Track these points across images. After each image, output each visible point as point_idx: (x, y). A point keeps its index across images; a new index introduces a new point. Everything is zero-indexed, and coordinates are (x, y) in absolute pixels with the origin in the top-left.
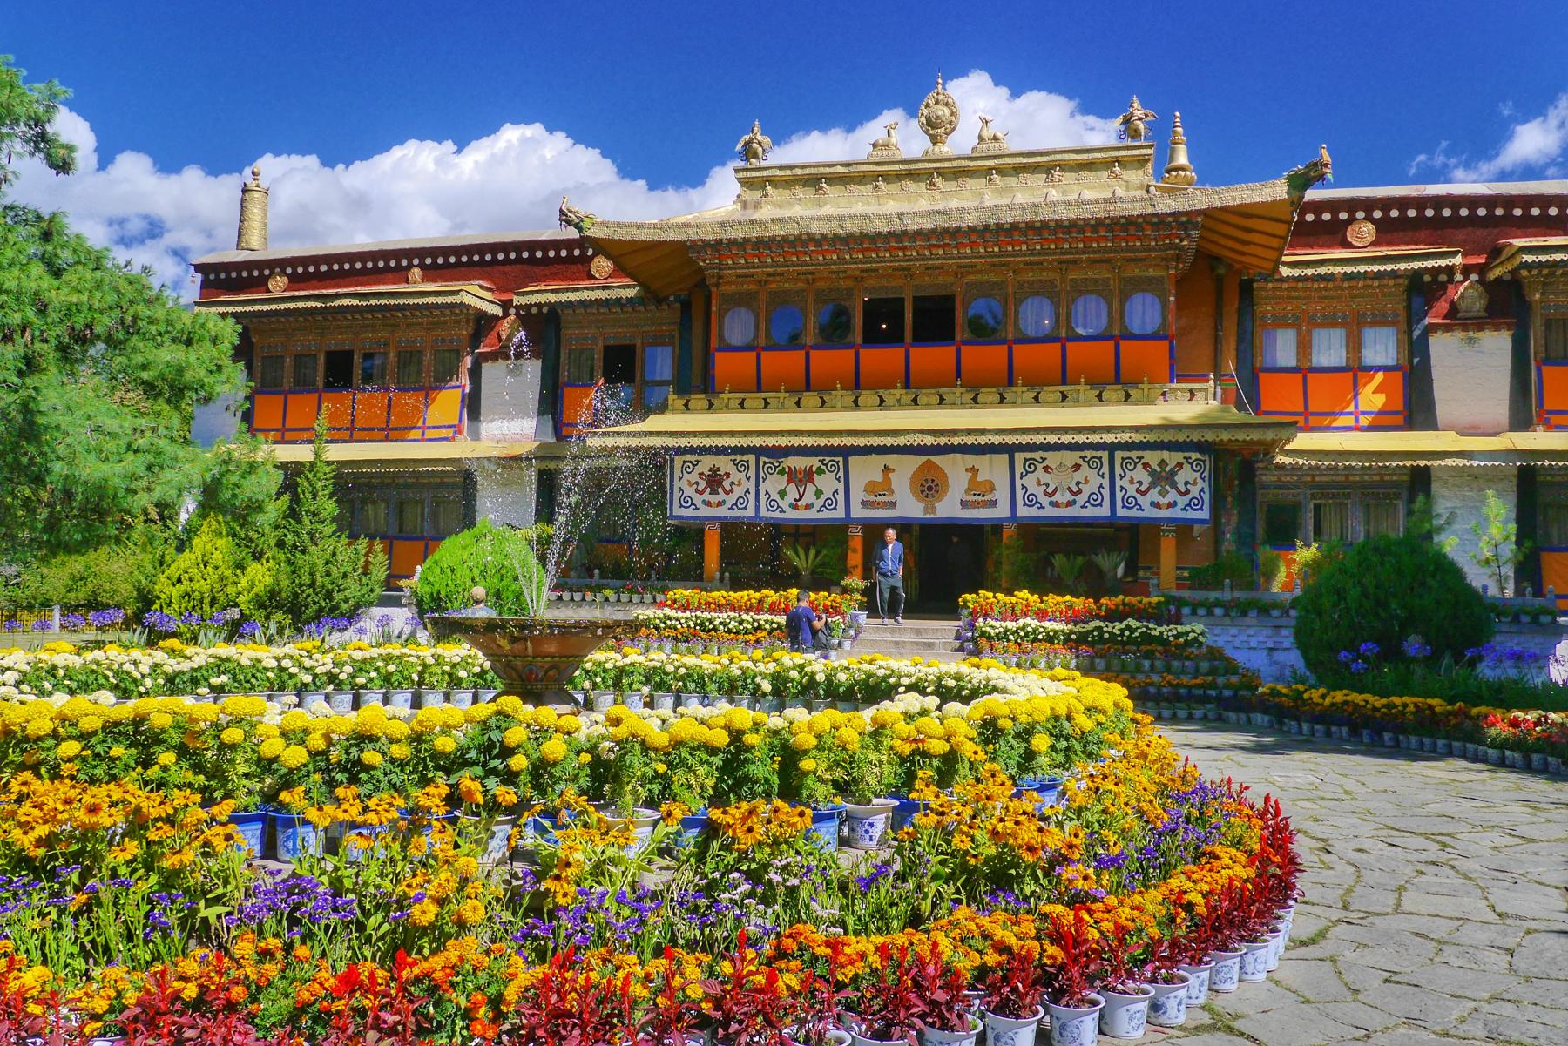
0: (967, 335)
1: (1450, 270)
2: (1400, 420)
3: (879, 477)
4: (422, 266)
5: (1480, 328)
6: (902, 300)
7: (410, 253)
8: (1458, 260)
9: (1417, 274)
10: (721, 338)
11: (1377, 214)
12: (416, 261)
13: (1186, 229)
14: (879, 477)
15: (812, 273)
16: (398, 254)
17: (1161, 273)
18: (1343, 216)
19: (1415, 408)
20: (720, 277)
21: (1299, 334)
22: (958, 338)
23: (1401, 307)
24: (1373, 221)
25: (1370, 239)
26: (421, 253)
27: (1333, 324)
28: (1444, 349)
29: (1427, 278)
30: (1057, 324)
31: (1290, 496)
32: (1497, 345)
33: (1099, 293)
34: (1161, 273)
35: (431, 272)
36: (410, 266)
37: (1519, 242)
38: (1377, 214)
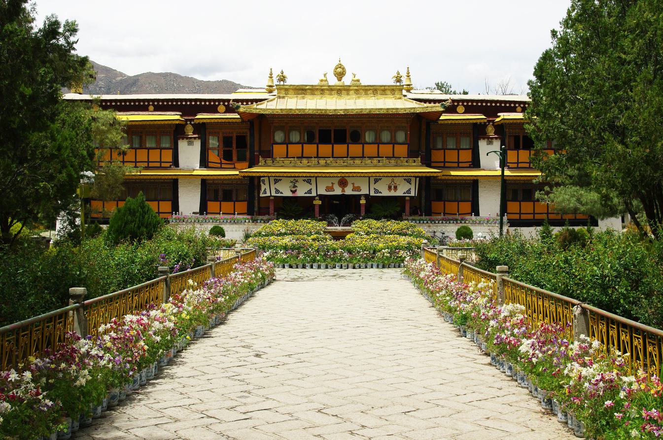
0: (350, 141)
3: (331, 185)
4: (153, 105)
8: (486, 121)
10: (274, 140)
11: (465, 104)
12: (151, 103)
17: (406, 125)
18: (456, 104)
19: (475, 163)
22: (347, 142)
28: (483, 145)
30: (376, 139)
32: (497, 145)
33: (388, 130)
34: (406, 125)
36: (149, 105)
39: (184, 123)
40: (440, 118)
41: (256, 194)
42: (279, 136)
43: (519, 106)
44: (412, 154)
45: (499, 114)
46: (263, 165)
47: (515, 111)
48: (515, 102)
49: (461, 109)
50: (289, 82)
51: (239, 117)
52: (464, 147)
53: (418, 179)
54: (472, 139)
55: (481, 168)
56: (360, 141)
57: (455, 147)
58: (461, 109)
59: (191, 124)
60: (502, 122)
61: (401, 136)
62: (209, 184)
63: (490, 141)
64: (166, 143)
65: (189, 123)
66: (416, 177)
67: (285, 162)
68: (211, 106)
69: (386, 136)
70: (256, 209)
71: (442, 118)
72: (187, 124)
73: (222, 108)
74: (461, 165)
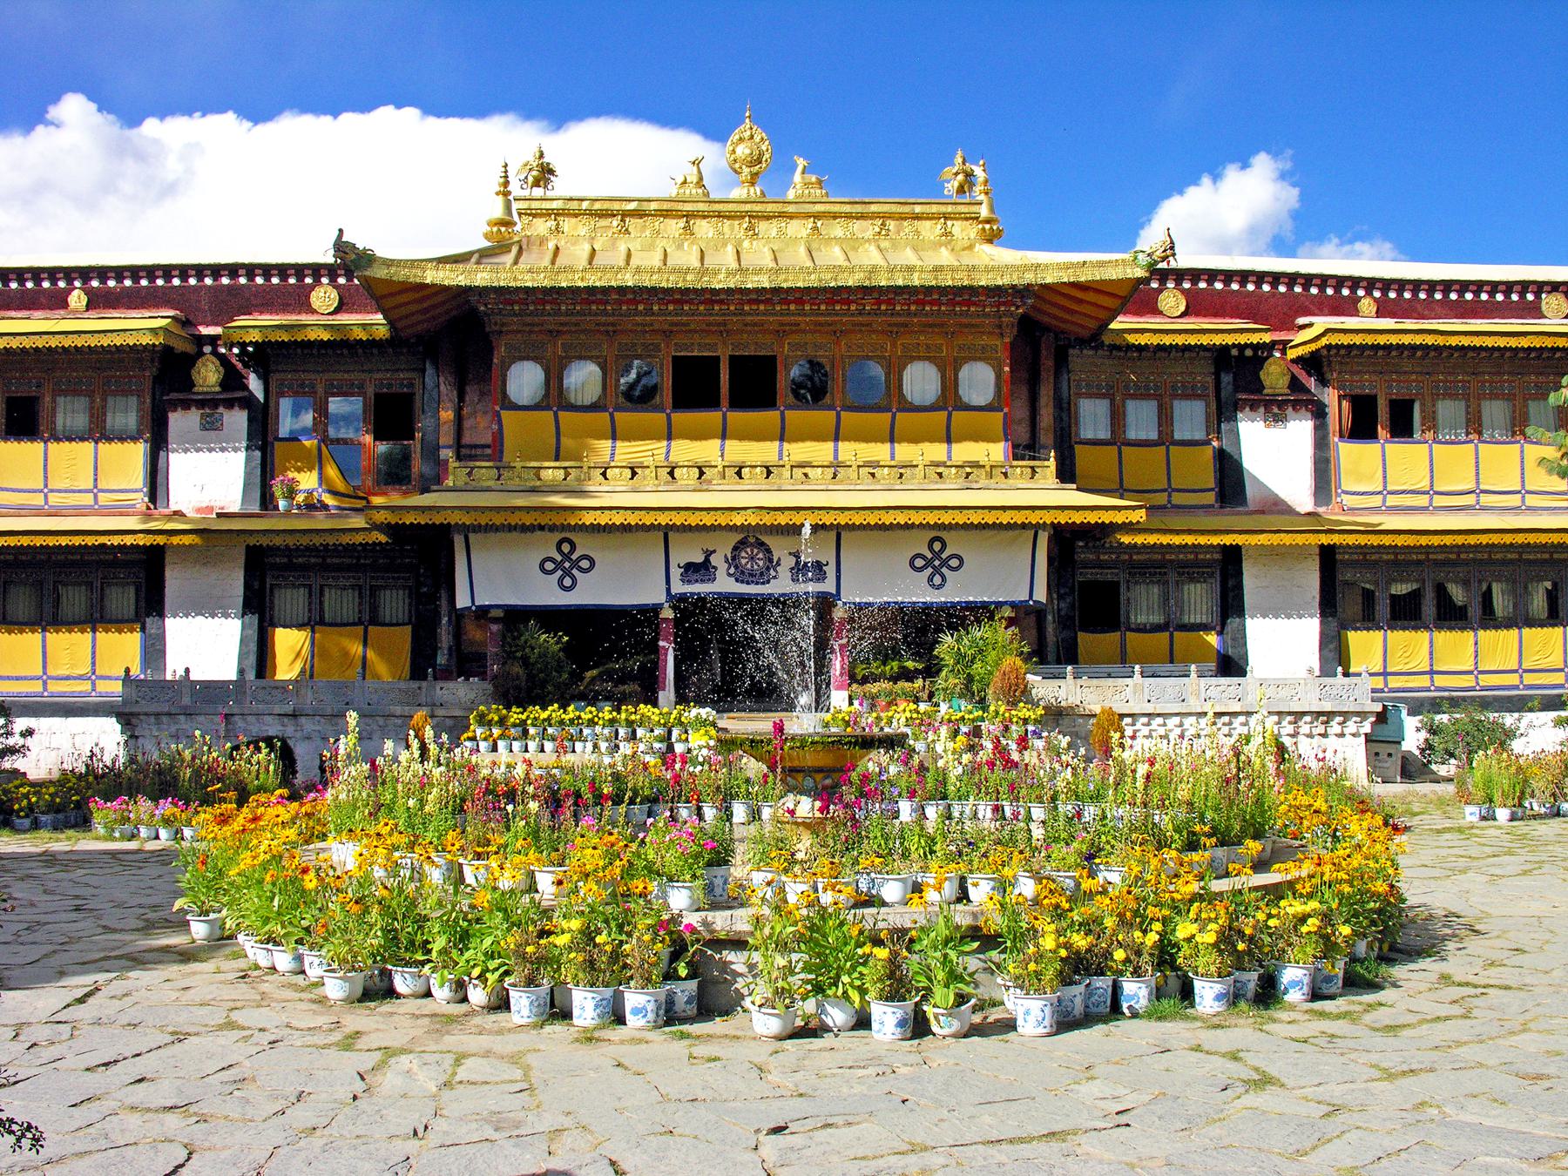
0: (791, 399)
1: (1256, 347)
2: (1210, 498)
4: (89, 292)
5: (1282, 405)
6: (717, 359)
7: (70, 273)
9: (1225, 349)
11: (1186, 285)
13: (1022, 297)
14: (700, 559)
15: (613, 324)
16: (53, 273)
20: (503, 325)
21: (1112, 404)
23: (1210, 379)
24: (1183, 291)
25: (1182, 308)
26: (85, 273)
27: (1145, 396)
29: (1234, 352)
31: (1108, 575)
35: (98, 301)
36: (69, 291)
37: (1321, 323)
38: (1186, 285)
39: (190, 348)
40: (1112, 326)
41: (444, 602)
42: (525, 380)
43: (1369, 293)
44: (1026, 449)
45: (1301, 321)
46: (460, 484)
47: (1354, 312)
48: (1355, 282)
49: (1172, 301)
50: (562, 187)
51: (379, 318)
52: (1187, 436)
53: (1043, 538)
54: (1214, 406)
55: (1251, 506)
56: (827, 400)
57: (1154, 436)
58: (1172, 301)
59: (215, 353)
60: (1324, 341)
61: (979, 382)
62: (274, 566)
63: (1275, 409)
64: (126, 414)
65: (207, 349)
66: (1037, 527)
67: (543, 474)
68: (285, 284)
69: (921, 381)
70: (441, 659)
71: (1112, 326)
72: (201, 354)
73: (324, 297)
74: (1178, 499)
